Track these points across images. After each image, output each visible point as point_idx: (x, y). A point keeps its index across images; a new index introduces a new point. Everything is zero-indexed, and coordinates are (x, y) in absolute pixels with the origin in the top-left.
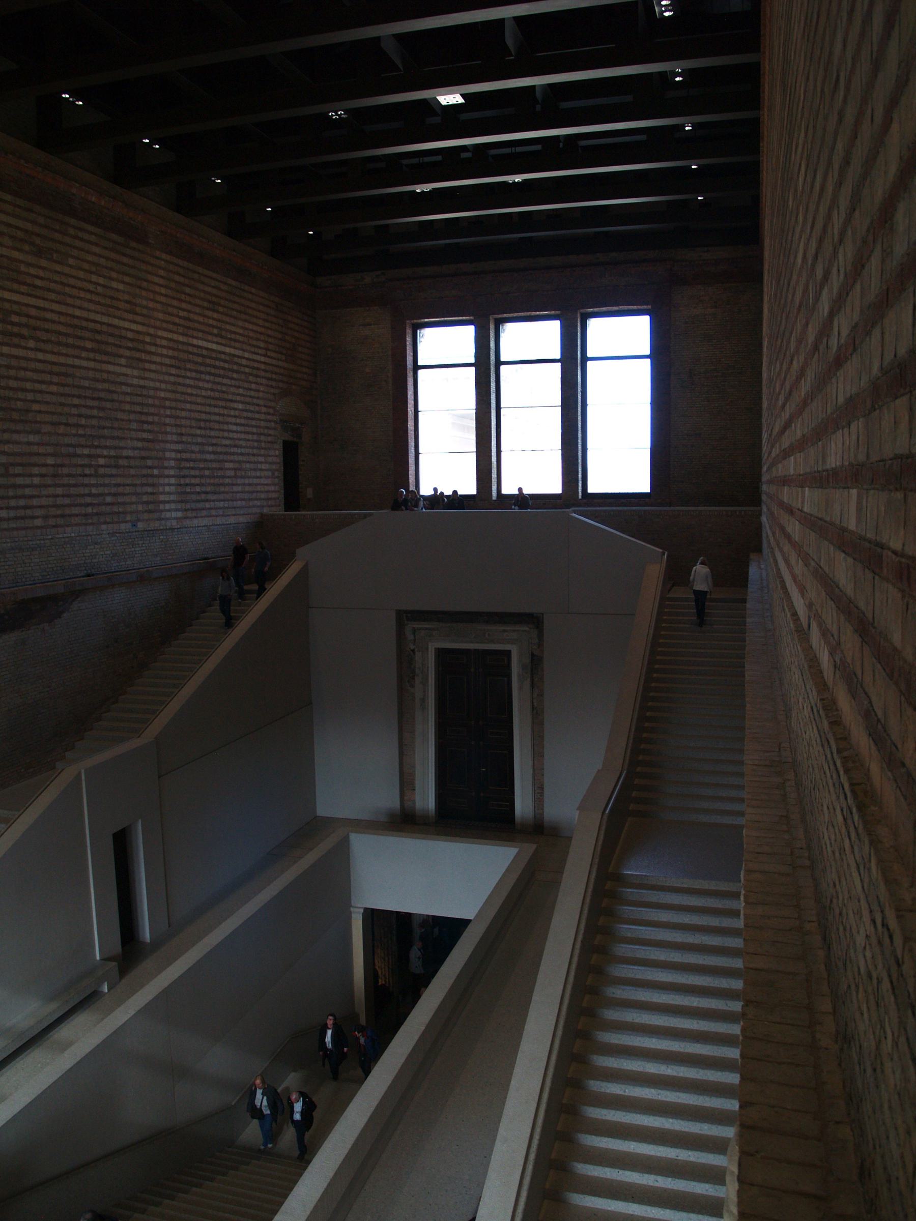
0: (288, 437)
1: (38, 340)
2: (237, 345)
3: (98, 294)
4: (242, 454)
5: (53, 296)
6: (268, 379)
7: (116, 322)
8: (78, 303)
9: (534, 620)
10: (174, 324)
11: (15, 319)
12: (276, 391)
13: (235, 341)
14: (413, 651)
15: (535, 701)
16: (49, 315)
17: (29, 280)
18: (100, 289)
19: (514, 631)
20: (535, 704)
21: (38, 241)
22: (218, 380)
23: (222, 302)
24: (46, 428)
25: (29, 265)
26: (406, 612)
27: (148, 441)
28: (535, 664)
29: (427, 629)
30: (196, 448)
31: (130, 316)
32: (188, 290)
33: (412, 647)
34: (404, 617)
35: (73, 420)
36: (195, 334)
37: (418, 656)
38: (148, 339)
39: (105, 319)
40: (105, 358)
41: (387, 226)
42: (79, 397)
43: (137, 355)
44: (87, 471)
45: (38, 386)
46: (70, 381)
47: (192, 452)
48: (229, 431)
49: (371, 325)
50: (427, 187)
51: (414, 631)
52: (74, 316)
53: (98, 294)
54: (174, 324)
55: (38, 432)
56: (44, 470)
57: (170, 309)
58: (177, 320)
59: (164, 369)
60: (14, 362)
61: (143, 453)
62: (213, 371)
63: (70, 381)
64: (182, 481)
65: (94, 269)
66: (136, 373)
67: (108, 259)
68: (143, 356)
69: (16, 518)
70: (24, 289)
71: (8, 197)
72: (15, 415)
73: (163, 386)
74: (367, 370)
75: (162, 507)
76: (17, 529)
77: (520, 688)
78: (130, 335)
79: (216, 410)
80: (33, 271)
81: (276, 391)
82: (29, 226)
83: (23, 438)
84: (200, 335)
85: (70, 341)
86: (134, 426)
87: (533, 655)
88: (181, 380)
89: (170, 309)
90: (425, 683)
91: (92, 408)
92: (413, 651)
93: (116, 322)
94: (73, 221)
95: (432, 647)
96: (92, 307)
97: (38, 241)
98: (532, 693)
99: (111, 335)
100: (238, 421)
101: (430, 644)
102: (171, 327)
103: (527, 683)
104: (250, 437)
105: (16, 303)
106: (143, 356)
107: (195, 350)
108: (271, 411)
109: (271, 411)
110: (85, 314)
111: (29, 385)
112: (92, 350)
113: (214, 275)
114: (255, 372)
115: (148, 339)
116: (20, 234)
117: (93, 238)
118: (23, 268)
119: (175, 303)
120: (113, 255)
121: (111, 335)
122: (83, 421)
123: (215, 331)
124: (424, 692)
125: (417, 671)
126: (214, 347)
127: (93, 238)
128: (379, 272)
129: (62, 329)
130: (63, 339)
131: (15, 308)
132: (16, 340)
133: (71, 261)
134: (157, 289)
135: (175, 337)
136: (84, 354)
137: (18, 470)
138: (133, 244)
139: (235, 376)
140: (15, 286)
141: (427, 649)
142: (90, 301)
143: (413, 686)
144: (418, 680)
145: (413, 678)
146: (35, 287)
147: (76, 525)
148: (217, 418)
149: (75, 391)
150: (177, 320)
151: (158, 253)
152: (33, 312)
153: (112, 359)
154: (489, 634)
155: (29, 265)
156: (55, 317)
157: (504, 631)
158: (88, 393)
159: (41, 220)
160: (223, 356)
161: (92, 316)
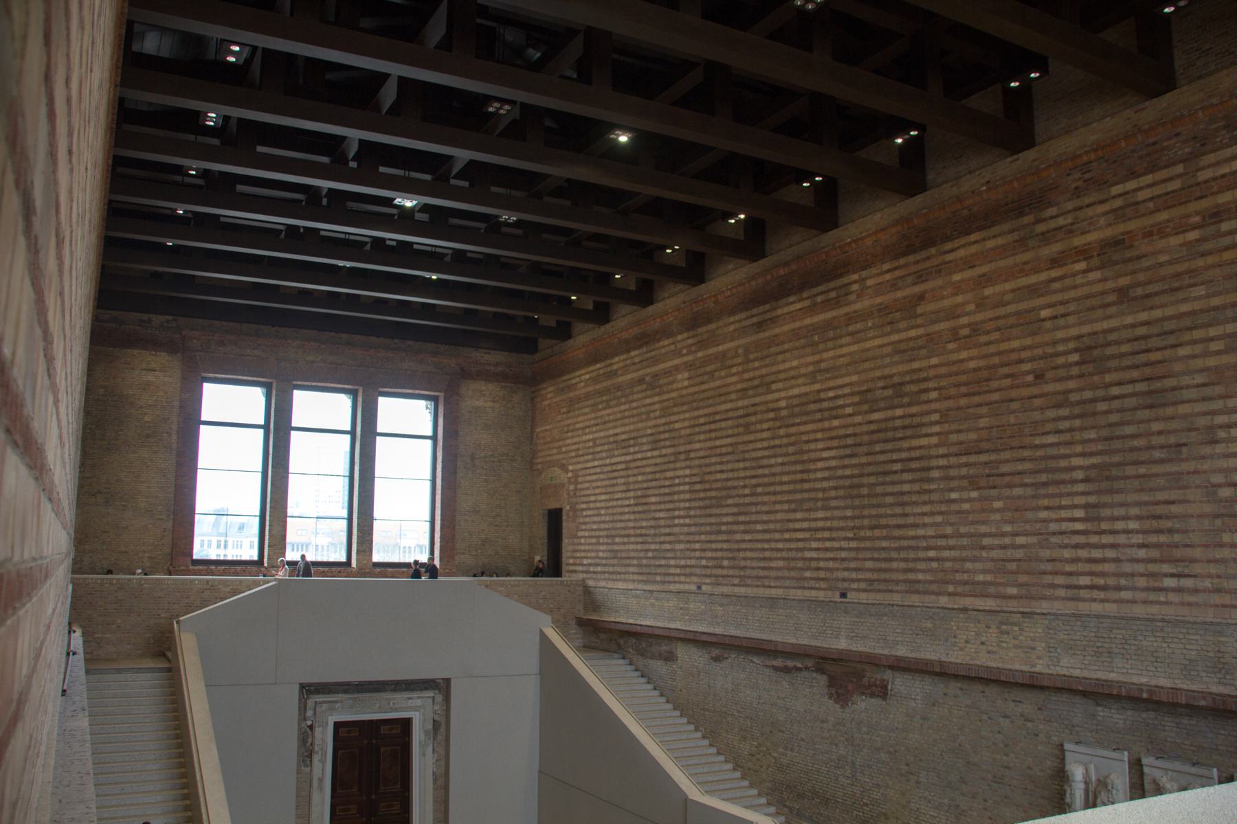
9: (442, 687)
14: (311, 727)
19: (419, 698)
26: (310, 685)
28: (440, 728)
29: (328, 702)
34: (308, 690)
41: (194, 276)
49: (155, 371)
50: (348, 264)
74: (147, 418)
87: (434, 721)
90: (323, 761)
95: (332, 720)
98: (433, 758)
128: (170, 318)
141: (327, 723)
144: (316, 758)
145: (310, 756)
154: (393, 703)
157: (410, 698)
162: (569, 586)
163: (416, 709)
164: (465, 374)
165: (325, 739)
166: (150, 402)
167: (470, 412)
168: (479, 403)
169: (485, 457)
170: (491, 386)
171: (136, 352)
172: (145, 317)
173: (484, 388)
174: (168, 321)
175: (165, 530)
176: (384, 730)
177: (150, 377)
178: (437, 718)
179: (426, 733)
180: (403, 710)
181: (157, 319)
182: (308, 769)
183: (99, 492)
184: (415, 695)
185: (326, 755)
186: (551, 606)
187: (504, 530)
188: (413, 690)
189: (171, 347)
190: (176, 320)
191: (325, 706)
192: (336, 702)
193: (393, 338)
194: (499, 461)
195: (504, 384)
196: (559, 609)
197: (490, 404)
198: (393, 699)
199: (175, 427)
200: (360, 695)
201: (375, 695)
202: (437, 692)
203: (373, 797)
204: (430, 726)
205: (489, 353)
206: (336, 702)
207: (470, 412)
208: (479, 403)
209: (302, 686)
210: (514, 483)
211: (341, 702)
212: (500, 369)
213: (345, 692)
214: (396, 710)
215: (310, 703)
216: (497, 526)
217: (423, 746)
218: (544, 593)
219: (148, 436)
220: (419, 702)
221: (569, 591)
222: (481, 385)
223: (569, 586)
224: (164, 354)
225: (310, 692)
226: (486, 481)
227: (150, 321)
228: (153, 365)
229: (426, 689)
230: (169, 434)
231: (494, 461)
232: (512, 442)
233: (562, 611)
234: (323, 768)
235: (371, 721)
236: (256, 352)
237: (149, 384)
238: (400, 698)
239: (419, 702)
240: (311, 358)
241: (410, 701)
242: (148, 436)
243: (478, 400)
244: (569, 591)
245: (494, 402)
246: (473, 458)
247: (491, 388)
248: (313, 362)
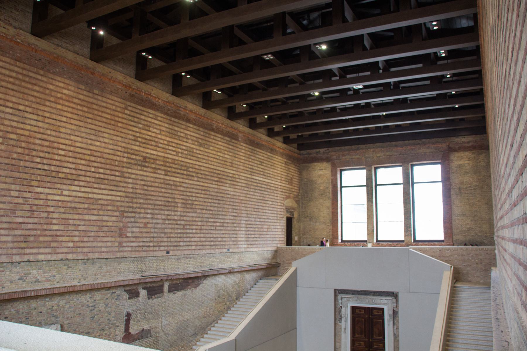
0: (289, 215)
1: (198, 177)
2: (270, 178)
3: (220, 160)
4: (270, 222)
5: (204, 161)
6: (282, 192)
7: (226, 170)
8: (213, 163)
9: (394, 295)
10: (247, 171)
11: (191, 170)
12: (284, 197)
13: (269, 177)
14: (341, 307)
15: (395, 331)
16: (202, 168)
17: (196, 155)
18: (221, 158)
20: (395, 333)
21: (200, 141)
22: (262, 192)
23: (265, 162)
24: (199, 211)
25: (197, 150)
27: (235, 216)
28: (395, 313)
29: (347, 298)
30: (253, 219)
31: (231, 168)
32: (252, 158)
33: (341, 305)
34: (337, 292)
35: (208, 208)
36: (254, 174)
37: (343, 309)
38: (237, 177)
39: (222, 169)
40: (221, 184)
42: (211, 199)
43: (233, 183)
44: (212, 228)
45: (197, 195)
46: (208, 193)
47: (252, 221)
48: (266, 213)
49: (322, 170)
50: (347, 117)
51: (342, 298)
52: (211, 168)
53: (220, 160)
54: (247, 171)
55: (196, 212)
56: (197, 227)
57: (246, 165)
58: (248, 169)
59: (242, 188)
60: (189, 186)
61: (233, 221)
62: (261, 189)
63: (208, 193)
64: (247, 233)
65: (219, 150)
66: (232, 190)
67: (224, 147)
68: (235, 183)
69: (186, 246)
70: (194, 158)
71: (191, 126)
72: (188, 206)
73: (242, 195)
74: (321, 188)
75: (239, 243)
76: (186, 250)
77: (389, 325)
78: (231, 175)
79: (261, 204)
80: (198, 152)
81: (284, 197)
82: (198, 136)
83: (190, 215)
84: (256, 175)
85: (209, 177)
86: (230, 210)
87: (394, 310)
88: (248, 192)
89: (246, 165)
90: (346, 321)
91: (215, 203)
92: (341, 307)
93: (226, 170)
94: (213, 133)
96: (218, 165)
97: (200, 141)
98: (394, 327)
99: (224, 175)
100: (269, 209)
101: (348, 304)
102: (246, 172)
103: (392, 323)
104: (274, 215)
105: (192, 164)
106: (235, 183)
107: (254, 181)
108: (282, 205)
109: (282, 205)
110: (215, 167)
111: (194, 195)
112: (217, 181)
113: (262, 151)
114: (276, 189)
115: (237, 177)
116: (194, 139)
117: (219, 139)
118: (195, 151)
119: (247, 162)
120: (226, 145)
121: (224, 175)
122: (212, 208)
123: (262, 173)
124: (346, 325)
125: (343, 316)
126: (261, 179)
127: (219, 139)
128: (326, 149)
129: (207, 173)
130: (207, 177)
131: (191, 166)
132: (190, 178)
133: (211, 148)
134: (241, 157)
135: (247, 175)
136: (214, 183)
137: (188, 227)
138: (233, 141)
139: (269, 191)
140: (192, 158)
141: (347, 306)
142: (217, 162)
143: (341, 322)
144: (343, 320)
145: (341, 319)
146: (198, 158)
147: (208, 249)
148: (261, 207)
149: (210, 197)
150: (248, 169)
151: (242, 144)
152: (197, 167)
153: (224, 184)
155: (197, 150)
156: (205, 169)
157: (381, 299)
158: (214, 198)
159: (202, 133)
160: (264, 183)
161: (218, 168)
162: (487, 251)
163: (384, 304)
164: (451, 150)
165: (347, 313)
166: (322, 182)
167: (456, 167)
168: (461, 162)
169: (466, 188)
170: (466, 153)
171: (315, 164)
172: (318, 150)
173: (463, 155)
174: (326, 150)
175: (330, 229)
176: (375, 312)
177: (321, 172)
178: (395, 309)
179: (390, 315)
180: (380, 304)
181: (322, 150)
182: (340, 324)
183: (307, 216)
184: (383, 298)
185: (347, 319)
186: (477, 261)
187: (479, 223)
188: (382, 296)
189: (327, 160)
190: (328, 149)
191: (345, 299)
192: (350, 298)
193: (415, 140)
194: (475, 189)
195: (474, 151)
196: (481, 262)
197: (467, 162)
198: (375, 299)
199: (331, 190)
200: (359, 296)
201: (365, 296)
202: (393, 297)
203: (371, 340)
204: (391, 313)
205: (464, 138)
206: (350, 298)
207: (456, 167)
208: (461, 162)
209: (335, 290)
210: (484, 199)
211: (352, 298)
212: (470, 144)
213: (353, 294)
214: (376, 304)
215: (340, 296)
216: (476, 221)
217: (389, 321)
218: (472, 254)
219: (322, 194)
220: (386, 301)
221: (487, 253)
222: (462, 154)
223: (487, 251)
224: (325, 163)
225: (339, 293)
226: (468, 199)
227: (319, 151)
228: (322, 168)
229: (388, 296)
230: (329, 193)
231: (471, 190)
232: (481, 179)
233: (483, 263)
234: (346, 324)
235: (369, 308)
236: (357, 156)
237: (321, 175)
238: (378, 299)
239: (386, 301)
240: (379, 155)
241: (382, 301)
242: (322, 194)
243: (460, 161)
244: (487, 253)
245: (469, 160)
246: (460, 189)
247: (467, 154)
248: (379, 157)
